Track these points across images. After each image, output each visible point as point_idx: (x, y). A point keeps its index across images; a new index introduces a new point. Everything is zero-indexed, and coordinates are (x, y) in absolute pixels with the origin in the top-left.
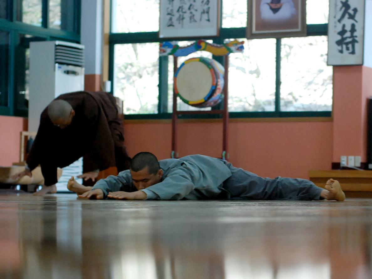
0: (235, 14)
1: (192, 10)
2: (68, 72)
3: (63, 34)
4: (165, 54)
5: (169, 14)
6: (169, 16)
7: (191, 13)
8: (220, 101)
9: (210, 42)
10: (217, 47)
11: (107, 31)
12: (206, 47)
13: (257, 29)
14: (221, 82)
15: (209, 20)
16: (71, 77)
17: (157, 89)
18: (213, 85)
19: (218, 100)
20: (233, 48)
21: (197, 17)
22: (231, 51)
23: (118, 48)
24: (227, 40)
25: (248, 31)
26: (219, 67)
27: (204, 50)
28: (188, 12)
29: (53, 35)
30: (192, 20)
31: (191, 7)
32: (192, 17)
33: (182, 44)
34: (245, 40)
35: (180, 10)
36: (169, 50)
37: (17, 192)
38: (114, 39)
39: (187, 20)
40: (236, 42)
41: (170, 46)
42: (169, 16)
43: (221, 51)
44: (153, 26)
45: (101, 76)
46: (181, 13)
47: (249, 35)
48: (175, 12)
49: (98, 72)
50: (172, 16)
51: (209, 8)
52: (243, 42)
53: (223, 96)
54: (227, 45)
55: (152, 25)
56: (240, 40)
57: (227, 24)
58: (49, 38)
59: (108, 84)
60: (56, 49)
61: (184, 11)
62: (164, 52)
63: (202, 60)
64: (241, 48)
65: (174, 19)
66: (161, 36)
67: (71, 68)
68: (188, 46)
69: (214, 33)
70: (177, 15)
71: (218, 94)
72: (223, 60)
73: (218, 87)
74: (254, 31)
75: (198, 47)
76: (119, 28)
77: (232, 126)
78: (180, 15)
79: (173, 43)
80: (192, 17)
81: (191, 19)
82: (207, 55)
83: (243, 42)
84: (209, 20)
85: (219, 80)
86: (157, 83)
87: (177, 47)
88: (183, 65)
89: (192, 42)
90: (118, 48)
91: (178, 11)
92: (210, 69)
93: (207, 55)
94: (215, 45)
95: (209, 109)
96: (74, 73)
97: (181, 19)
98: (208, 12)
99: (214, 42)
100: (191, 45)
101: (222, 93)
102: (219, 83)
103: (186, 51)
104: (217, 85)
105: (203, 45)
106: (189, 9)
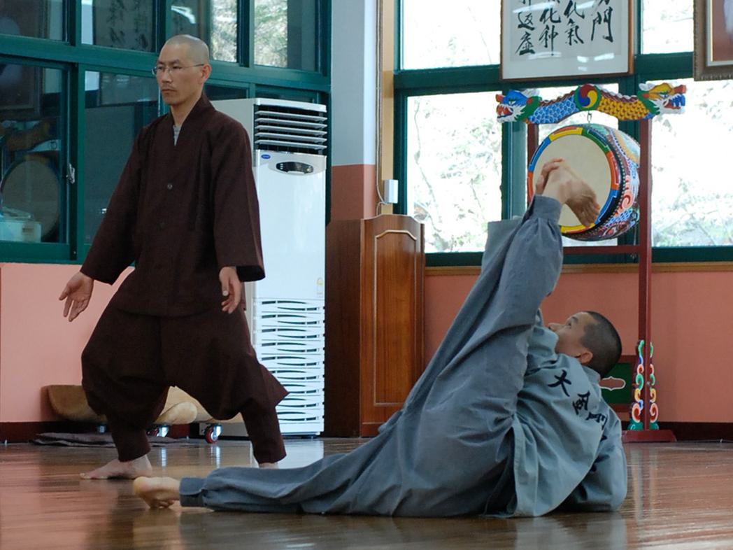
0: (668, 28)
1: (573, 16)
2: (288, 167)
3: (292, 77)
4: (511, 119)
5: (520, 26)
6: (523, 31)
7: (571, 21)
8: (633, 223)
9: (613, 88)
10: (623, 100)
11: (389, 67)
12: (599, 99)
13: (714, 59)
14: (633, 182)
15: (610, 38)
16: (295, 177)
17: (499, 194)
18: (612, 190)
19: (628, 222)
20: (659, 103)
21: (585, 32)
22: (655, 112)
23: (415, 104)
24: (647, 86)
25: (698, 61)
26: (629, 146)
27: (595, 108)
28: (565, 19)
29: (259, 83)
30: (574, 38)
31: (572, 8)
32: (573, 32)
33: (548, 94)
34: (688, 82)
35: (548, 14)
36: (518, 110)
37: (162, 442)
38: (407, 85)
39: (562, 37)
40: (665, 89)
41: (518, 101)
42: (524, 30)
43: (635, 110)
44: (486, 55)
45: (377, 168)
46: (549, 23)
47: (699, 71)
48: (536, 22)
49: (368, 159)
50: (529, 31)
51: (611, 10)
52: (681, 89)
53: (638, 212)
54: (644, 96)
55: (482, 50)
56: (675, 83)
57: (653, 44)
58: (253, 89)
59: (394, 185)
60: (257, 116)
61: (555, 18)
62: (508, 113)
63: (590, 132)
64: (677, 102)
65: (535, 36)
66: (509, 74)
67: (298, 157)
68: (559, 99)
69: (622, 67)
70: (540, 27)
71: (626, 208)
72: (638, 129)
73: (626, 193)
74: (711, 62)
75: (581, 102)
76: (420, 56)
77: (663, 282)
78: (547, 27)
79: (528, 93)
80: (573, 32)
81: (570, 36)
82: (605, 121)
83: (681, 89)
84: (610, 38)
85: (627, 177)
86: (500, 183)
87: (536, 102)
88: (547, 141)
89: (575, 88)
90: (415, 104)
91: (543, 16)
92: (606, 152)
93: (605, 121)
94: (620, 96)
95: (614, 242)
96: (305, 168)
97: (550, 36)
98: (608, 21)
99: (620, 91)
100: (572, 92)
101: (635, 206)
102: (627, 185)
103: (558, 111)
104: (622, 188)
105: (592, 96)
106: (567, 13)
